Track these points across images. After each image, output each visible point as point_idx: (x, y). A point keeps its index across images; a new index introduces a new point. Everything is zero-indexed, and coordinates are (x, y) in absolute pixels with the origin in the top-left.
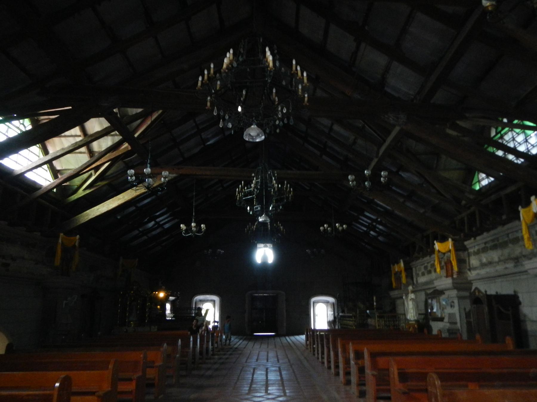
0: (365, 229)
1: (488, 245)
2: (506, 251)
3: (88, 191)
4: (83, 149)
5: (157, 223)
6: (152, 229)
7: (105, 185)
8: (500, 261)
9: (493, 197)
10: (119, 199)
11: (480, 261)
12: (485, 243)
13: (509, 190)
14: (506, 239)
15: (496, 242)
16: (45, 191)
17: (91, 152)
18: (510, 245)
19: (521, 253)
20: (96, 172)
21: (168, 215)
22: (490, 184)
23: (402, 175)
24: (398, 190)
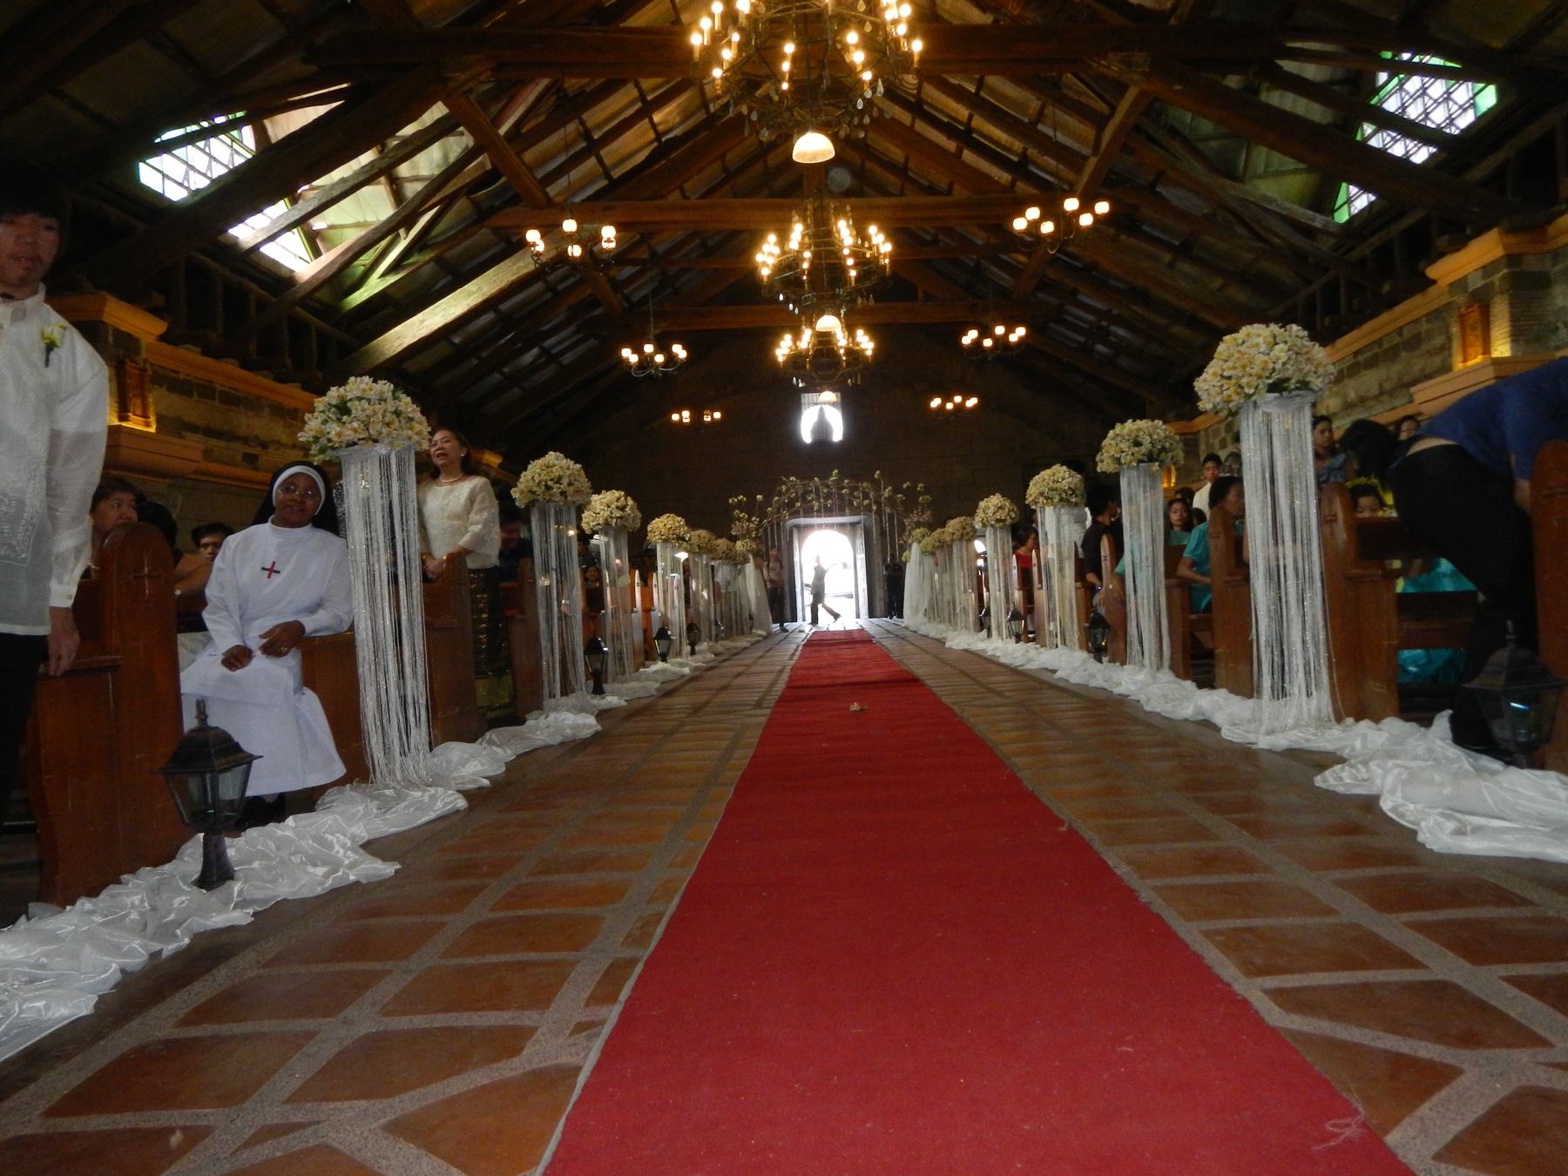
0: (1082, 339)
1: (1360, 358)
2: (1396, 369)
3: (392, 279)
4: (382, 179)
5: (545, 351)
6: (534, 368)
7: (428, 262)
8: (1382, 393)
9: (1375, 241)
10: (470, 294)
11: (1345, 396)
12: (1356, 353)
13: (1407, 222)
14: (1397, 340)
15: (1377, 350)
16: (309, 288)
17: (396, 186)
18: (1404, 354)
19: (1423, 369)
20: (408, 232)
21: (572, 328)
22: (1371, 204)
23: (1165, 193)
24: (1156, 233)
